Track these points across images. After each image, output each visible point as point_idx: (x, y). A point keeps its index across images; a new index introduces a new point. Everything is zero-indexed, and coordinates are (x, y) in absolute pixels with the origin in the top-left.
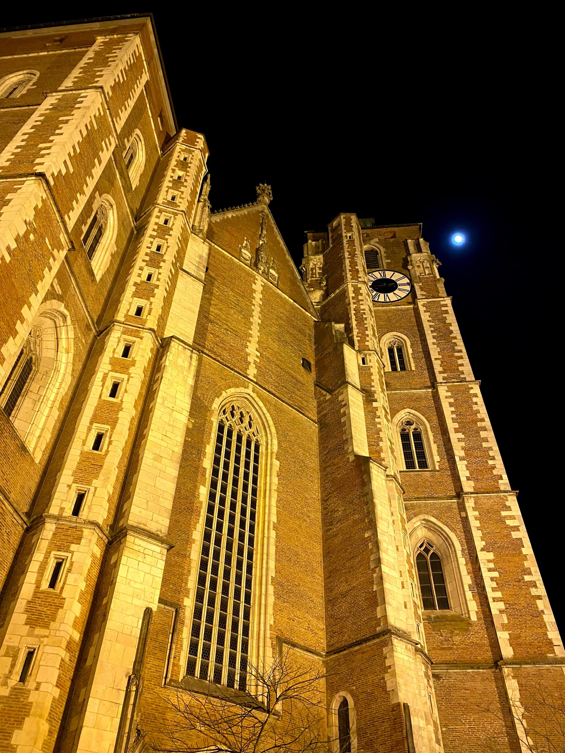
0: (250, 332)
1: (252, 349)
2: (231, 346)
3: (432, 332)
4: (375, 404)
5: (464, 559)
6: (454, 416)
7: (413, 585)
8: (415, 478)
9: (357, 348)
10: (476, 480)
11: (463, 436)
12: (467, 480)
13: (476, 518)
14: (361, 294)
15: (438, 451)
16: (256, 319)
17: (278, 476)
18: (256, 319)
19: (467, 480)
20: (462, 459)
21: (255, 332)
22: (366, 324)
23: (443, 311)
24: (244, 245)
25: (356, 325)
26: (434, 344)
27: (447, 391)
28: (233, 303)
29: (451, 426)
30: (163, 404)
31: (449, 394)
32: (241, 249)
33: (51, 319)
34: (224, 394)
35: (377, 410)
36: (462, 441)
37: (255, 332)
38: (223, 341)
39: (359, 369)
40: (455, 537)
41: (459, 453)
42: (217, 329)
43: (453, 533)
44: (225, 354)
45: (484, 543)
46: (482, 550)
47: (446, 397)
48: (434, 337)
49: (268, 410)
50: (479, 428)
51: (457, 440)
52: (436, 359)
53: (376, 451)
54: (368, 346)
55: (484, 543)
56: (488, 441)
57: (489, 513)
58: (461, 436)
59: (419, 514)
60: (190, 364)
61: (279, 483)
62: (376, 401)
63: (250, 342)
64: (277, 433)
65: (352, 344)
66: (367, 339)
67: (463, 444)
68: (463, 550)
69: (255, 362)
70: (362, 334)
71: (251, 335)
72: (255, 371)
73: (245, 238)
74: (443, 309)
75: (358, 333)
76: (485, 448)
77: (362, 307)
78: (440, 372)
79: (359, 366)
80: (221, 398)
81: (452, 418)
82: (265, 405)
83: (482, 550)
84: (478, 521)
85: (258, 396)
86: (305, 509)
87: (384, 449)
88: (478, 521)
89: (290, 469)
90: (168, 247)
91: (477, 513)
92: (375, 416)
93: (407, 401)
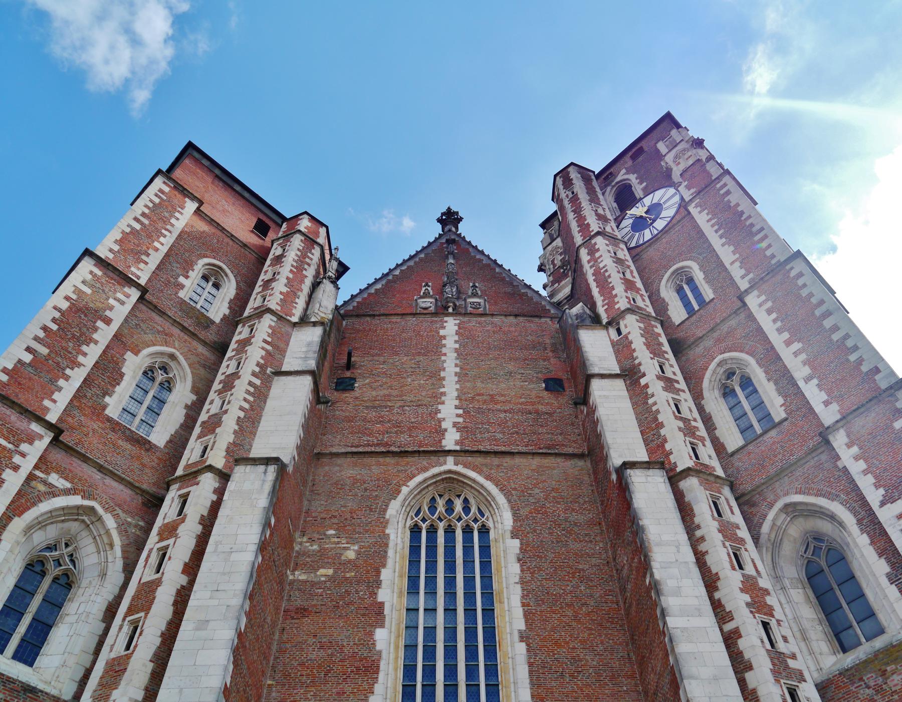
2: (412, 423)
3: (716, 231)
4: (643, 381)
5: (865, 535)
6: (779, 324)
7: (773, 623)
8: (757, 451)
9: (605, 321)
10: (840, 399)
11: (800, 345)
12: (826, 406)
13: (856, 458)
14: (598, 250)
15: (778, 390)
17: (519, 560)
19: (826, 406)
20: (807, 380)
21: (451, 388)
22: (611, 283)
23: (723, 194)
25: (599, 292)
26: (723, 245)
27: (758, 297)
29: (777, 340)
30: (215, 551)
31: (763, 298)
32: (416, 300)
33: (76, 520)
34: (405, 490)
35: (648, 387)
36: (801, 353)
37: (451, 388)
38: (398, 425)
39: (613, 347)
40: (840, 506)
41: (799, 371)
43: (835, 503)
44: (404, 438)
45: (882, 491)
46: (883, 504)
47: (760, 305)
48: (721, 237)
49: (488, 478)
50: (820, 317)
51: (793, 356)
53: (658, 446)
55: (882, 491)
56: (839, 329)
57: (875, 437)
58: (796, 346)
59: (776, 501)
60: (264, 481)
61: (522, 571)
62: (644, 375)
63: (443, 403)
64: (509, 501)
65: (596, 320)
66: (616, 300)
67: (803, 356)
68: (859, 522)
69: (455, 425)
71: (444, 394)
72: (457, 436)
74: (722, 192)
76: (837, 341)
77: (601, 265)
78: (743, 277)
79: (612, 342)
80: (401, 498)
81: (778, 330)
82: (480, 472)
83: (883, 504)
84: (862, 461)
85: (465, 466)
86: (583, 588)
87: (667, 436)
88: (862, 461)
89: (542, 541)
90: (246, 358)
91: (855, 450)
92: (647, 397)
93: (715, 346)
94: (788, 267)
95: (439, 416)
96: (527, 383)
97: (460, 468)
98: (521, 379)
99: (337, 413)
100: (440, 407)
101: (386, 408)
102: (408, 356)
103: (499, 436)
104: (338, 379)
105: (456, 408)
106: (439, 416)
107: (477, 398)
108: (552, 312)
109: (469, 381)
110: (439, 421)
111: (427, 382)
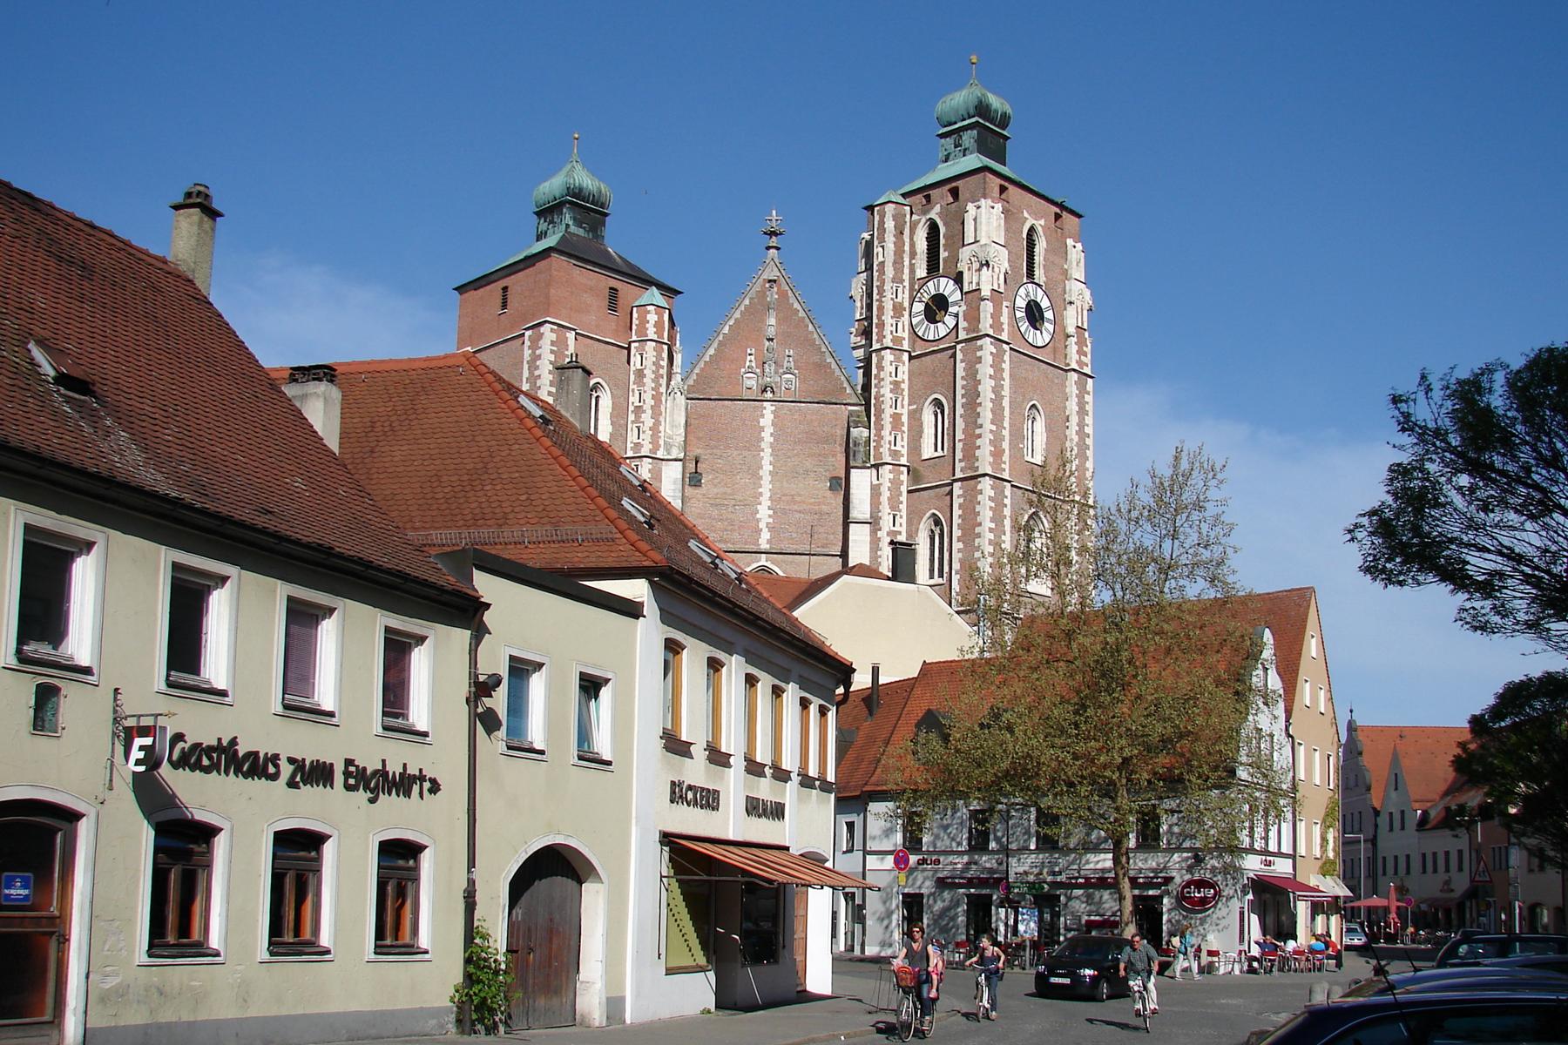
0: (760, 490)
1: (764, 513)
2: (741, 522)
16: (767, 467)
18: (767, 467)
21: (766, 488)
24: (748, 364)
27: (960, 488)
37: (766, 488)
44: (736, 536)
52: (960, 441)
54: (881, 453)
63: (760, 504)
73: (749, 351)
79: (871, 482)
85: (772, 563)
94: (979, 479)
95: (758, 516)
97: (768, 564)
99: (693, 509)
100: (759, 507)
103: (794, 535)
106: (758, 516)
107: (783, 498)
108: (848, 392)
109: (778, 481)
110: (758, 521)
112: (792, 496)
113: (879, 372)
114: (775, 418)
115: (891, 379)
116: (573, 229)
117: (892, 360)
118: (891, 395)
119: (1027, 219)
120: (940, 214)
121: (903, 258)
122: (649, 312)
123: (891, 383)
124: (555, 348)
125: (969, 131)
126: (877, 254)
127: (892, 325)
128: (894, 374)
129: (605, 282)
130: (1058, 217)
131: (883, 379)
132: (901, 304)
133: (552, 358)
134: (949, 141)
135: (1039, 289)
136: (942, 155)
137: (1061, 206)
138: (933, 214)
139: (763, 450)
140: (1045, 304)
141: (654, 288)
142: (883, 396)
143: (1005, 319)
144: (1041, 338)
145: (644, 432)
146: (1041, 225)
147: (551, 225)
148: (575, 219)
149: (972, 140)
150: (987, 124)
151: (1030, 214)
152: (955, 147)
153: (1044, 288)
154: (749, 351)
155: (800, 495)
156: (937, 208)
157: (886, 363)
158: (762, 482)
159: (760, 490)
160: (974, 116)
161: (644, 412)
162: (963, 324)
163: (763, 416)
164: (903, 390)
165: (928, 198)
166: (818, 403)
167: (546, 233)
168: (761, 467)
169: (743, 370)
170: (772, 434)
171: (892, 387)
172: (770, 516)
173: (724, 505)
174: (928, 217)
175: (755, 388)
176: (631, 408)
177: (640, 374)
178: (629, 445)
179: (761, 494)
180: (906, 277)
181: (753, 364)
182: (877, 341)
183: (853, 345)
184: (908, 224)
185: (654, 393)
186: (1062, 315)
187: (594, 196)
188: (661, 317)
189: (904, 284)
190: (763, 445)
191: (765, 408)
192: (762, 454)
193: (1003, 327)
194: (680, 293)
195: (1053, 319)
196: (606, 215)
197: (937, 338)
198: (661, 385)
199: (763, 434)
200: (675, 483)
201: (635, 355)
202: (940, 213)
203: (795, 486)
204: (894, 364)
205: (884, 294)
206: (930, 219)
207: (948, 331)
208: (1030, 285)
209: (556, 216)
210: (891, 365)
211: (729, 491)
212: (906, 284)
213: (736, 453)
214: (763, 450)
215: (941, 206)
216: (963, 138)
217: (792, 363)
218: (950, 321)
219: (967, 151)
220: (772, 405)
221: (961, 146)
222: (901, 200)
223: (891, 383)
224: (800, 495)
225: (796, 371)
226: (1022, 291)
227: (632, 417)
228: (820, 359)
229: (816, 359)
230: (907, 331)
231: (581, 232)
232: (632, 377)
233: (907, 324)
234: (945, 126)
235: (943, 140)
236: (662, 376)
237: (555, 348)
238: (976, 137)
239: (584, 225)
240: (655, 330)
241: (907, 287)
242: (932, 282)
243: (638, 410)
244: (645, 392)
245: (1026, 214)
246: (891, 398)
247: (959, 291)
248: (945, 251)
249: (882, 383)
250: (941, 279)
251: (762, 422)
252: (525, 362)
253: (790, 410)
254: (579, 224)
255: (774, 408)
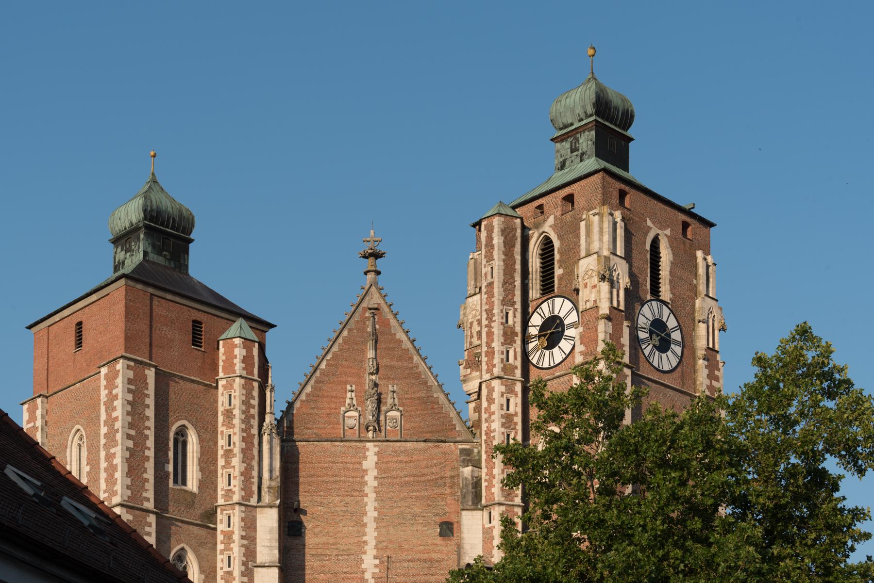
0: (365, 538)
16: (371, 513)
18: (371, 513)
21: (371, 535)
24: (348, 401)
28: (341, 513)
37: (371, 535)
42: (327, 562)
70: (490, 476)
73: (349, 388)
75: (486, 475)
96: (426, 528)
98: (422, 523)
100: (364, 557)
101: (326, 557)
102: (339, 496)
104: (289, 523)
105: (374, 558)
110: (364, 571)
111: (354, 529)
112: (399, 543)
113: (489, 405)
114: (379, 459)
115: (504, 412)
116: (153, 257)
117: (504, 391)
118: (503, 430)
119: (650, 228)
120: (553, 227)
121: (513, 278)
122: (236, 346)
123: (502, 416)
124: (133, 387)
125: (587, 133)
126: (486, 274)
127: (502, 353)
128: (505, 407)
129: (187, 313)
130: (685, 226)
131: (494, 413)
132: (512, 329)
133: (130, 397)
134: (567, 145)
135: (664, 307)
136: (557, 162)
137: (688, 213)
138: (548, 227)
139: (366, 495)
140: (672, 323)
141: (243, 321)
142: (494, 431)
143: (625, 340)
144: (668, 360)
145: (235, 478)
146: (666, 235)
147: (128, 254)
148: (154, 246)
149: (590, 143)
150: (607, 123)
151: (654, 223)
152: (572, 152)
153: (670, 306)
154: (349, 388)
155: (408, 543)
156: (551, 220)
157: (496, 395)
158: (366, 530)
159: (365, 538)
160: (591, 115)
161: (234, 456)
162: (580, 348)
163: (365, 458)
164: (516, 424)
165: (540, 207)
166: (425, 441)
167: (123, 262)
168: (365, 514)
169: (343, 409)
170: (376, 478)
171: (504, 420)
172: (376, 566)
173: (326, 555)
174: (541, 231)
175: (357, 428)
176: (221, 452)
177: (229, 414)
178: (220, 492)
179: (365, 543)
180: (518, 298)
181: (355, 402)
182: (487, 372)
183: (462, 378)
184: (519, 239)
185: (245, 435)
186: (691, 336)
187: (174, 219)
188: (249, 350)
189: (516, 306)
190: (367, 490)
191: (368, 450)
192: (366, 499)
193: (624, 349)
194: (275, 326)
195: (680, 340)
196: (191, 241)
197: (552, 365)
198: (252, 427)
199: (366, 478)
200: (271, 531)
201: (222, 394)
202: (554, 225)
203: (403, 533)
204: (505, 395)
205: (494, 319)
206: (544, 232)
207: (564, 356)
208: (654, 303)
209: (133, 244)
210: (502, 396)
211: (331, 540)
212: (518, 306)
213: (337, 499)
214: (366, 495)
215: (555, 218)
216: (581, 141)
217: (396, 400)
218: (565, 345)
219: (585, 157)
220: (375, 446)
221: (578, 150)
222: (510, 212)
223: (502, 416)
224: (408, 543)
225: (401, 408)
226: (646, 309)
227: (221, 462)
228: (426, 394)
229: (422, 394)
230: (519, 359)
231: (160, 260)
232: (221, 419)
233: (519, 350)
234: (561, 129)
235: (558, 145)
236: (253, 417)
237: (133, 387)
238: (594, 139)
239: (164, 253)
240: (243, 365)
241: (519, 310)
242: (546, 303)
243: (228, 454)
244: (235, 434)
245: (649, 223)
246: (503, 433)
247: (575, 312)
248: (560, 267)
249: (493, 417)
250: (556, 299)
251: (366, 465)
252: (102, 404)
253: (394, 451)
254: (159, 251)
255: (377, 449)
